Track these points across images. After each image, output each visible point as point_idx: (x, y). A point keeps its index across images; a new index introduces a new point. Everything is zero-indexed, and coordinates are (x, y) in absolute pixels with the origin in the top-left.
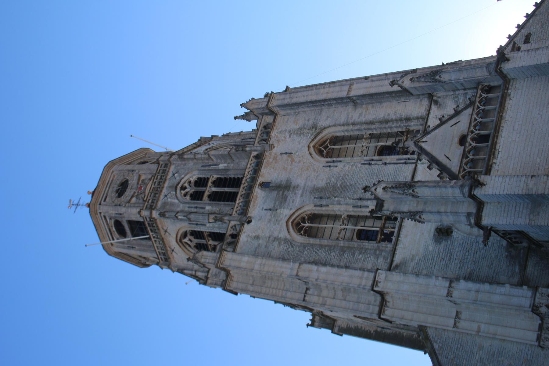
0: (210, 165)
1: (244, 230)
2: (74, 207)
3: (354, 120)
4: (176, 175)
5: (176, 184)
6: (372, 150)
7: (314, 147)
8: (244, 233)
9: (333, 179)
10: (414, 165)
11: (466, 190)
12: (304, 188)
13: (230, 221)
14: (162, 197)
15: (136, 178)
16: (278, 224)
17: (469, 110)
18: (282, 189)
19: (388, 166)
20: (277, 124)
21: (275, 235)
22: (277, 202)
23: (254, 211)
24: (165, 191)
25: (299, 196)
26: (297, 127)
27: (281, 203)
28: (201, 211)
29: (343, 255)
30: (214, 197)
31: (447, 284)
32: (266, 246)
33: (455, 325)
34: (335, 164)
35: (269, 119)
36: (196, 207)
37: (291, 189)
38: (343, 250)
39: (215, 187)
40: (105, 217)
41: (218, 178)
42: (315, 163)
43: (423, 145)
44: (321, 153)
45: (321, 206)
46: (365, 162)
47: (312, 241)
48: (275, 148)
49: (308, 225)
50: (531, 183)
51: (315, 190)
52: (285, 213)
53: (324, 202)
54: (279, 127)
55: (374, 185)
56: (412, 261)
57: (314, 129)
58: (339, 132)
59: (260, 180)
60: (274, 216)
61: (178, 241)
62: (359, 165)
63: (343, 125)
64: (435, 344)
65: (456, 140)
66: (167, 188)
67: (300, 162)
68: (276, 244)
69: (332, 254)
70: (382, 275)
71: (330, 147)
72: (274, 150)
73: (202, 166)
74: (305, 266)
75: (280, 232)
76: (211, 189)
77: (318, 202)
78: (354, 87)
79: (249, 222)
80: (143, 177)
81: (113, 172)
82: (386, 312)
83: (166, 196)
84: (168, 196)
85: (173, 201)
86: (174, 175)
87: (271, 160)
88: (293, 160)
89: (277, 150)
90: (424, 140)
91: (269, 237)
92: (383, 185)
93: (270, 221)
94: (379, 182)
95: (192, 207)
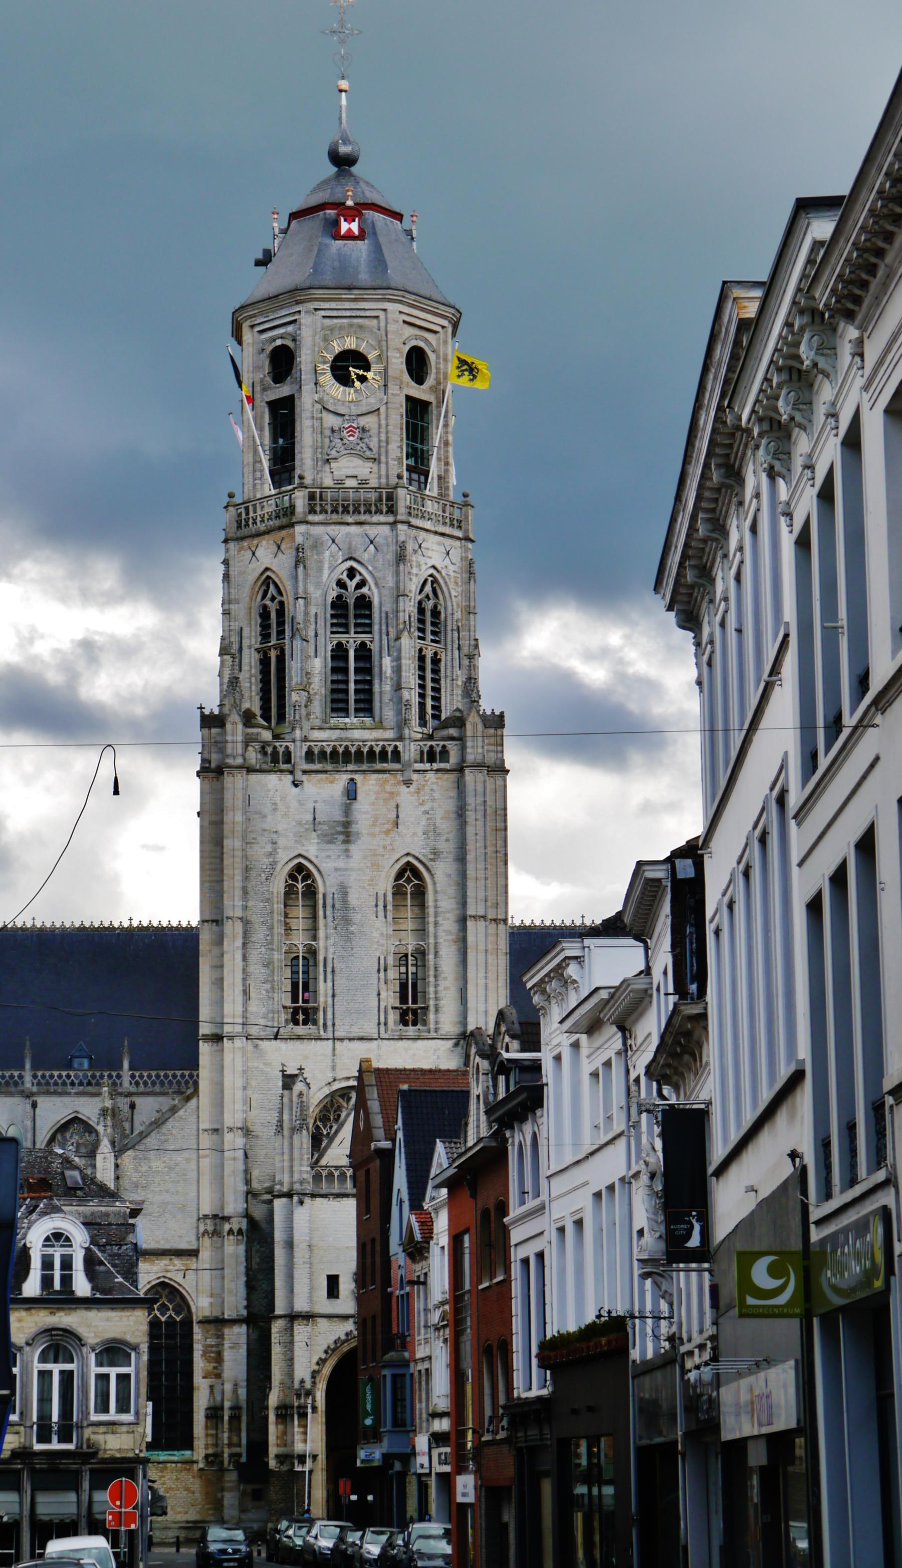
0: (388, 635)
1: (283, 777)
3: (442, 924)
4: (372, 547)
5: (356, 556)
7: (408, 863)
8: (280, 780)
9: (358, 916)
10: (376, 1036)
11: (297, 1187)
12: (346, 870)
13: (294, 741)
14: (333, 530)
16: (296, 841)
18: (344, 832)
19: (377, 999)
20: (446, 776)
21: (281, 842)
22: (326, 827)
24: (344, 529)
25: (336, 865)
26: (439, 822)
27: (326, 835)
28: (312, 653)
29: (265, 966)
30: (339, 653)
31: (240, 1125)
32: (264, 830)
35: (454, 758)
36: (316, 635)
37: (343, 847)
38: (268, 964)
39: (356, 651)
40: (294, 321)
41: (370, 650)
42: (383, 874)
44: (400, 875)
45: (324, 906)
46: (382, 962)
47: (279, 907)
48: (408, 790)
50: (304, 1246)
51: (344, 891)
52: (311, 849)
53: (329, 912)
54: (440, 783)
55: (305, 1079)
56: (264, 1064)
57: (432, 857)
59: (358, 778)
60: (307, 829)
61: (268, 573)
62: (378, 954)
63: (436, 907)
64: (183, 1110)
66: (347, 534)
67: (385, 847)
68: (269, 848)
69: (263, 950)
70: (239, 1043)
71: (409, 888)
72: (403, 788)
73: (387, 613)
74: (239, 927)
75: (286, 848)
77: (329, 902)
81: (385, 310)
82: (206, 1044)
83: (333, 541)
84: (334, 546)
86: (372, 542)
87: (388, 788)
88: (387, 832)
91: (276, 832)
92: (305, 1092)
93: (300, 824)
94: (308, 1084)
95: (316, 623)
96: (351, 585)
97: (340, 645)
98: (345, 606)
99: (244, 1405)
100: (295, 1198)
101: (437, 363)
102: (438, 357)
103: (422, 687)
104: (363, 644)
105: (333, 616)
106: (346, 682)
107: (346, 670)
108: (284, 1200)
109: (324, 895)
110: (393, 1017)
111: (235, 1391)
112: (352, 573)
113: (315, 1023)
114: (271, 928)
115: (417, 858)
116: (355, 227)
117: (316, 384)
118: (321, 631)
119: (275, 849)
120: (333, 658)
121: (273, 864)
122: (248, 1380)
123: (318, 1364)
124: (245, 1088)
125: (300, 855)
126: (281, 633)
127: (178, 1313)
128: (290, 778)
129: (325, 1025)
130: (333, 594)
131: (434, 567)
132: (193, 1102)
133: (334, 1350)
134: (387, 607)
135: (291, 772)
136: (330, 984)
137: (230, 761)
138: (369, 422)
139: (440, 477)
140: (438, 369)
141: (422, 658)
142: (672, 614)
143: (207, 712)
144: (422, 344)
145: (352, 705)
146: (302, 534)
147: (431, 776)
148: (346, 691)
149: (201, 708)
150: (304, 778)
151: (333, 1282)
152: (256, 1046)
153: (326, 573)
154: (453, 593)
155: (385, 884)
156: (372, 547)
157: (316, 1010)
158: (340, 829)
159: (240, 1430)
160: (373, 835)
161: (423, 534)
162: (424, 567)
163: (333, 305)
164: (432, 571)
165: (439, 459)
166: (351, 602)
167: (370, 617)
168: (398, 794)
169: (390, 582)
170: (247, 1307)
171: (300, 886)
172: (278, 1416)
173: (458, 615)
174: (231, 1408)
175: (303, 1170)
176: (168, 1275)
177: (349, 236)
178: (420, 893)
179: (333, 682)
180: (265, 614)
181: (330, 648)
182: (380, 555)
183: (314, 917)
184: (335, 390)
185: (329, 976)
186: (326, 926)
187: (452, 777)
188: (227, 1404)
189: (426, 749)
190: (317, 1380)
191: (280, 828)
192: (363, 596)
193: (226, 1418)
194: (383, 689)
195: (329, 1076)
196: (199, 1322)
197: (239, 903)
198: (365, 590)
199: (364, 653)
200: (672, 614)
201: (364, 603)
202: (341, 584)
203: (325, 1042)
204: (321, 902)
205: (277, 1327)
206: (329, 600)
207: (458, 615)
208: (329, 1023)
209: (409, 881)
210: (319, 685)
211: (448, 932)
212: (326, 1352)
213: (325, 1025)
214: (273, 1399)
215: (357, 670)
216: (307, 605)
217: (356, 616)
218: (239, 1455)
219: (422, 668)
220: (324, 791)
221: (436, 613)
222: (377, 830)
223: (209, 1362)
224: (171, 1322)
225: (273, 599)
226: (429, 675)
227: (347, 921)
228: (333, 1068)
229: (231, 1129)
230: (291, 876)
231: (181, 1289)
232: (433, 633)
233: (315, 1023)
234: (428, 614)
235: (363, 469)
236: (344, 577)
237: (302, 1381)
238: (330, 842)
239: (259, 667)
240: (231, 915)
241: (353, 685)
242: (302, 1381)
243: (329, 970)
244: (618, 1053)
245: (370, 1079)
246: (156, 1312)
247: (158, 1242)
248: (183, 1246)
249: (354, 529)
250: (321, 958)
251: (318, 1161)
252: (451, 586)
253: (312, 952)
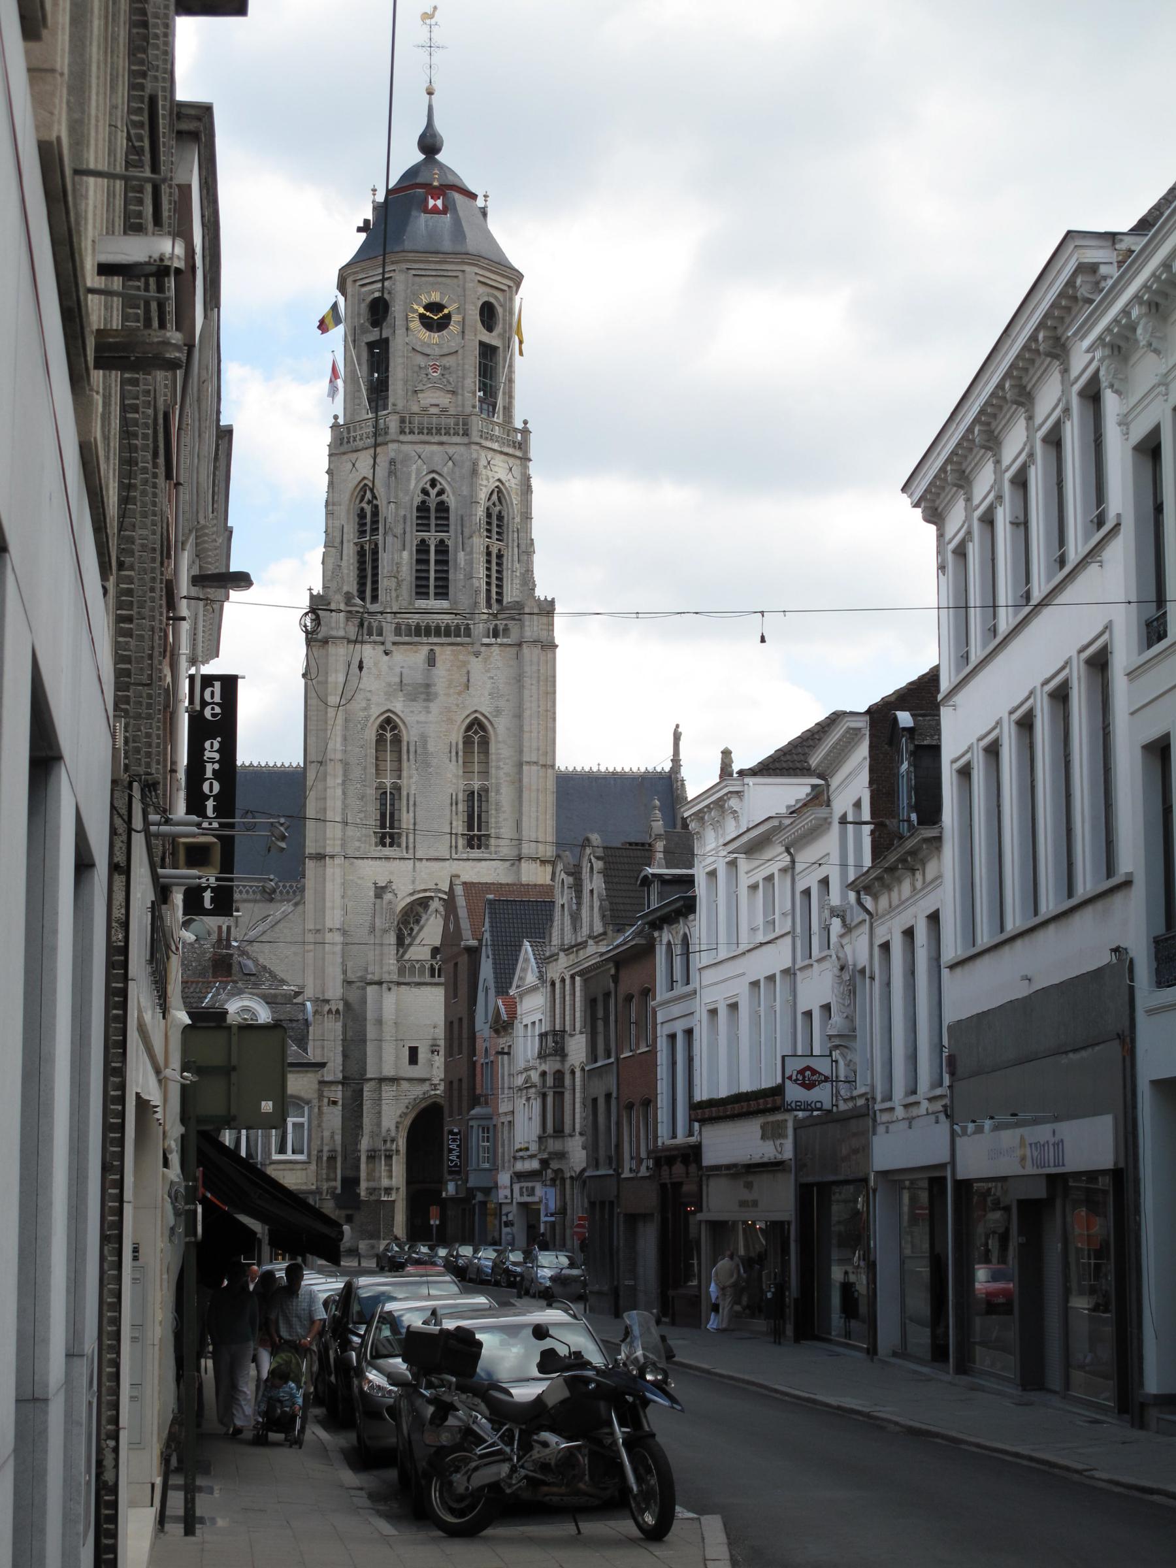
14: (419, 448)
15: (453, 345)
18: (424, 692)
21: (374, 699)
24: (428, 448)
34: (454, 758)
37: (425, 704)
51: (424, 739)
52: (398, 706)
59: (437, 649)
62: (451, 791)
67: (457, 705)
68: (364, 704)
72: (473, 659)
77: (412, 749)
85: (413, 476)
87: (461, 657)
88: (459, 694)
89: (476, 665)
93: (389, 685)
96: (433, 493)
97: (423, 541)
98: (428, 510)
99: (339, 1148)
100: (385, 985)
101: (504, 316)
102: (505, 311)
103: (488, 576)
104: (442, 541)
105: (418, 518)
106: (428, 571)
107: (427, 562)
108: (375, 987)
110: (461, 842)
111: (332, 1137)
112: (433, 483)
113: (399, 846)
114: (365, 768)
116: (439, 203)
117: (407, 329)
118: (408, 529)
119: (369, 705)
120: (418, 551)
121: (367, 718)
122: (343, 1129)
124: (343, 897)
125: (389, 711)
126: (375, 530)
128: (382, 648)
129: (407, 847)
130: (418, 498)
131: (499, 480)
132: (300, 907)
136: (411, 814)
137: (334, 633)
138: (449, 361)
139: (504, 408)
140: (504, 320)
141: (489, 554)
142: (919, 511)
143: (315, 593)
144: (492, 300)
145: (432, 590)
146: (395, 451)
147: (496, 650)
148: (428, 579)
149: (310, 589)
150: (393, 648)
151: (413, 1052)
152: (352, 864)
153: (413, 483)
154: (515, 502)
156: (450, 463)
157: (400, 834)
158: (422, 690)
159: (336, 1168)
160: (448, 695)
161: (490, 455)
162: (491, 480)
163: (422, 266)
164: (497, 483)
165: (504, 393)
166: (433, 507)
167: (447, 519)
168: (469, 662)
170: (343, 1071)
171: (388, 735)
172: (368, 1157)
173: (517, 520)
175: (391, 961)
177: (435, 210)
178: (485, 743)
179: (417, 571)
180: (362, 515)
181: (415, 543)
182: (457, 469)
183: (400, 760)
184: (424, 334)
185: (411, 809)
186: (409, 767)
187: (514, 650)
188: (326, 1148)
189: (491, 627)
191: (373, 689)
192: (442, 503)
193: (325, 1158)
194: (456, 577)
195: (410, 889)
197: (339, 746)
198: (444, 497)
199: (442, 549)
200: (919, 511)
201: (443, 508)
202: (425, 492)
204: (404, 749)
205: (367, 1088)
206: (415, 504)
207: (517, 520)
208: (411, 846)
209: (476, 733)
210: (407, 572)
211: (507, 774)
213: (407, 847)
214: (365, 1144)
215: (437, 562)
216: (397, 509)
217: (437, 518)
218: (336, 1188)
219: (489, 562)
220: (410, 659)
221: (500, 517)
222: (452, 691)
225: (369, 502)
226: (494, 567)
227: (428, 765)
228: (413, 882)
229: (331, 930)
230: (382, 727)
232: (498, 533)
233: (399, 846)
234: (494, 517)
235: (444, 400)
236: (428, 486)
237: (389, 1130)
238: (414, 700)
239: (356, 557)
240: (333, 757)
241: (433, 573)
242: (389, 1130)
243: (411, 803)
244: (783, 870)
245: (459, 890)
249: (435, 448)
250: (404, 793)
251: (402, 956)
252: (513, 496)
253: (397, 788)
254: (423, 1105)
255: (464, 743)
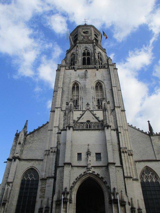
2: (84, 21)
6: (98, 98)
14: (83, 45)
17: (97, 121)
21: (72, 79)
23: (78, 71)
24: (85, 45)
30: (84, 59)
33: (49, 130)
35: (106, 67)
43: (87, 111)
45: (81, 88)
49: (76, 86)
50: (69, 142)
51: (85, 86)
52: (78, 80)
58: (103, 87)
59: (88, 70)
65: (88, 120)
70: (59, 109)
72: (97, 71)
74: (61, 89)
76: (86, 57)
78: (115, 88)
79: (75, 71)
80: (89, 37)
88: (94, 77)
90: (89, 111)
97: (84, 57)
98: (85, 53)
104: (88, 57)
109: (81, 87)
111: (48, 201)
112: (86, 49)
114: (69, 92)
115: (100, 81)
121: (70, 82)
123: (73, 184)
125: (76, 81)
127: (35, 178)
130: (83, 52)
133: (79, 179)
134: (92, 52)
135: (74, 69)
136: (81, 101)
138: (89, 37)
151: (79, 155)
155: (94, 85)
169: (92, 49)
171: (76, 86)
174: (45, 208)
176: (34, 166)
178: (101, 87)
185: (82, 100)
187: (106, 69)
190: (73, 190)
192: (88, 52)
196: (41, 180)
197: (62, 85)
203: (80, 111)
209: (99, 85)
211: (108, 92)
212: (76, 179)
223: (42, 193)
224: (33, 180)
231: (37, 171)
237: (66, 188)
242: (66, 188)
243: (81, 98)
246: (29, 177)
247: (33, 157)
248: (39, 158)
249: (86, 44)
254: (84, 178)
255: (96, 87)
